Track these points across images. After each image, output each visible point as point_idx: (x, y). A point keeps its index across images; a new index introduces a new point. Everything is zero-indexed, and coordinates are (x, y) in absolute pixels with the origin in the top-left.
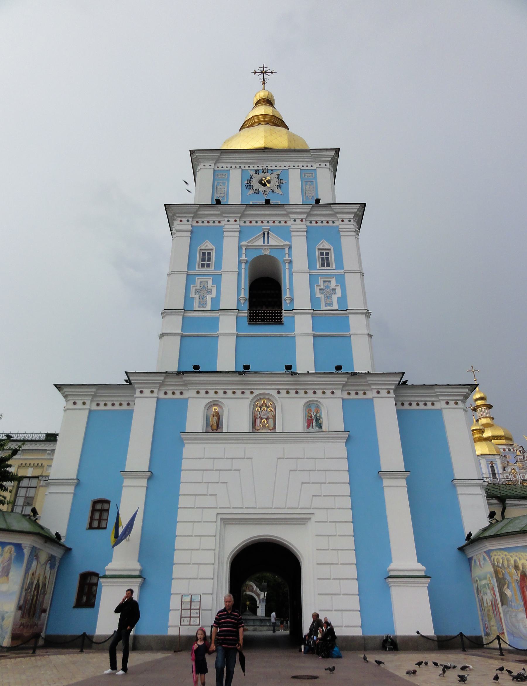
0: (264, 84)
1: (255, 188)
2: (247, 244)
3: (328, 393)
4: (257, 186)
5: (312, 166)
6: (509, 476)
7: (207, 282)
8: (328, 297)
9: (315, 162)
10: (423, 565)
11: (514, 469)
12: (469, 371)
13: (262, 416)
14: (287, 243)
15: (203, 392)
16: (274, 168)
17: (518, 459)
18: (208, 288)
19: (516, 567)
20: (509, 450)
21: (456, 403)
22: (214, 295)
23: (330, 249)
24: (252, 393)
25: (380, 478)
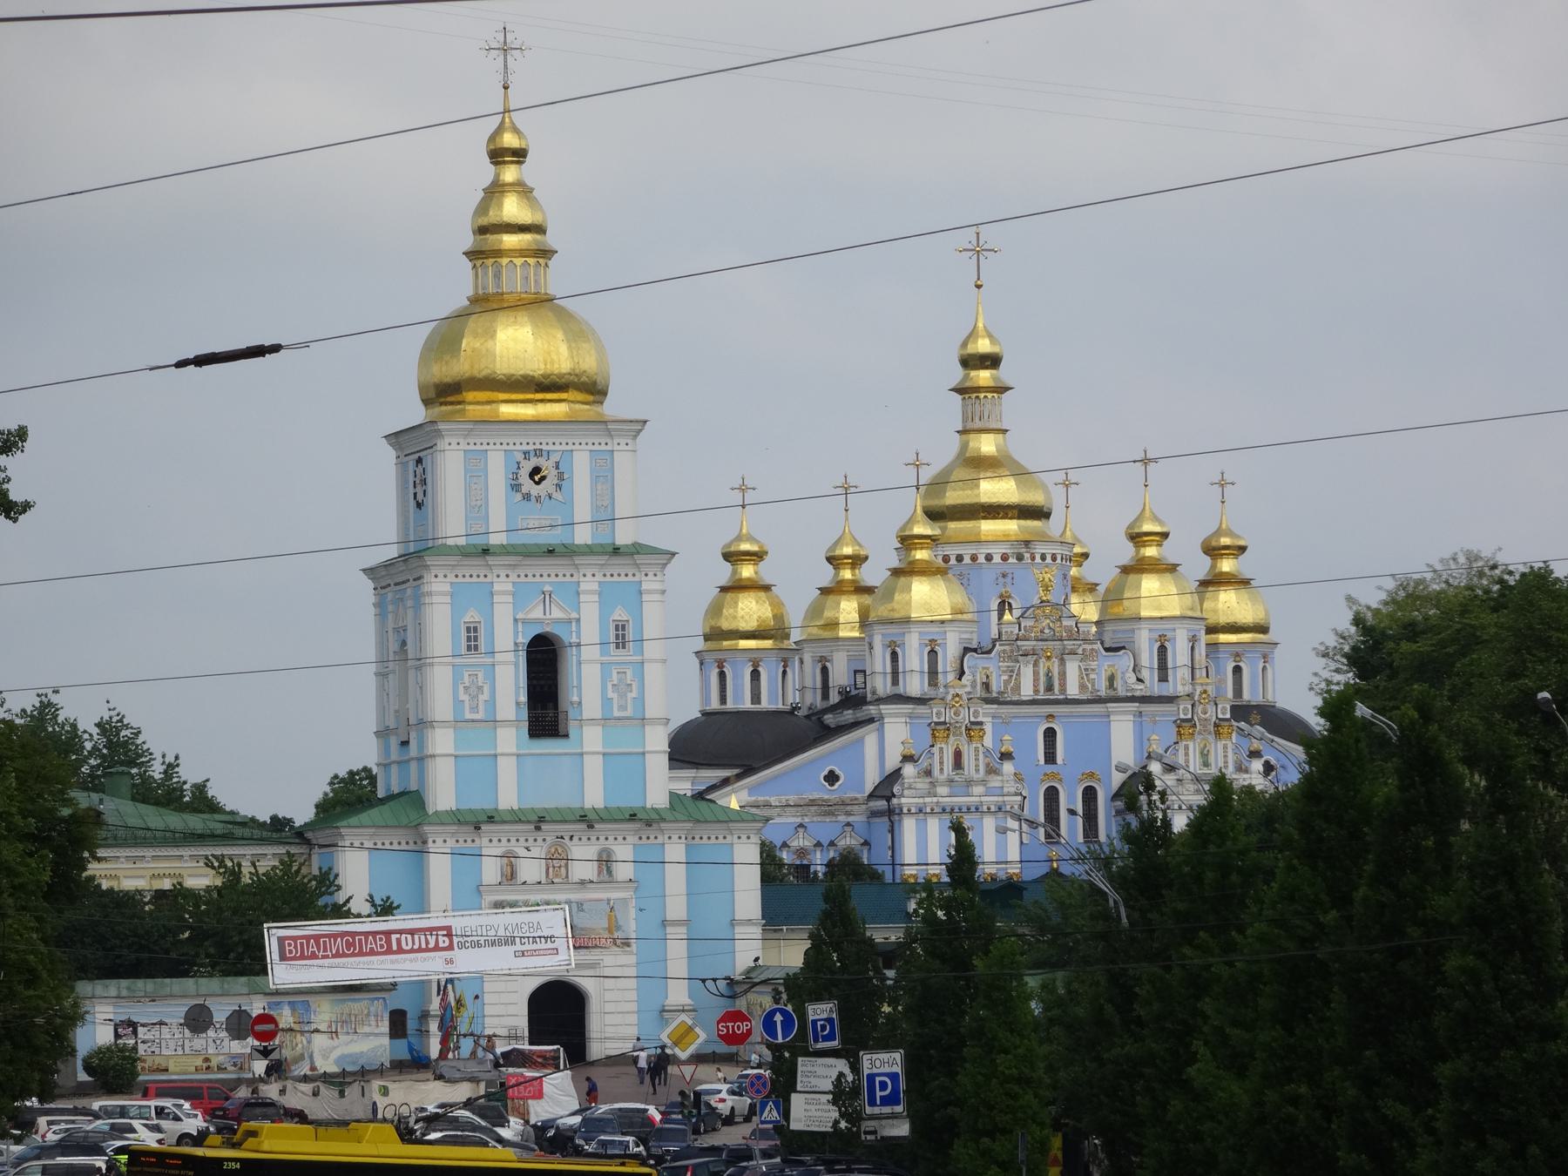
0: (506, 88)
1: (524, 490)
2: (524, 617)
3: (620, 838)
4: (528, 485)
5: (606, 444)
7: (476, 675)
8: (622, 696)
9: (611, 437)
10: (693, 1000)
11: (957, 695)
12: (965, 250)
13: (556, 865)
14: (574, 615)
15: (495, 840)
16: (551, 447)
18: (480, 684)
19: (761, 1006)
20: (1020, 558)
21: (749, 838)
22: (485, 696)
23: (628, 621)
24: (544, 840)
25: (665, 926)
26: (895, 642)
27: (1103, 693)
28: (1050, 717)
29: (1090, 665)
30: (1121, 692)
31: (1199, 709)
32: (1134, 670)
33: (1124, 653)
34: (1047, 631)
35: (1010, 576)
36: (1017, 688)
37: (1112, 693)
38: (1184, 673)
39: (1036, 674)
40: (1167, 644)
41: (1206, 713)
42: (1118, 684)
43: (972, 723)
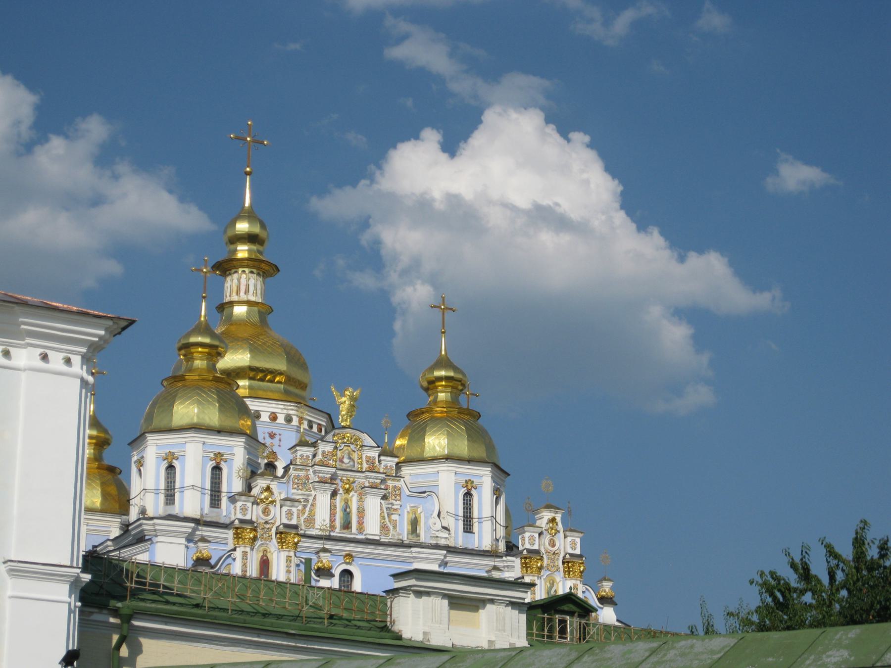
6: (250, 509)
11: (268, 489)
17: (298, 457)
20: (289, 419)
26: (172, 454)
27: (405, 537)
28: (349, 556)
29: (393, 504)
30: (423, 539)
31: (546, 538)
32: (439, 516)
33: (428, 495)
34: (346, 460)
35: (277, 437)
36: (310, 521)
37: (414, 539)
38: (487, 526)
39: (333, 508)
40: (473, 492)
41: (554, 546)
42: (421, 529)
43: (286, 526)
